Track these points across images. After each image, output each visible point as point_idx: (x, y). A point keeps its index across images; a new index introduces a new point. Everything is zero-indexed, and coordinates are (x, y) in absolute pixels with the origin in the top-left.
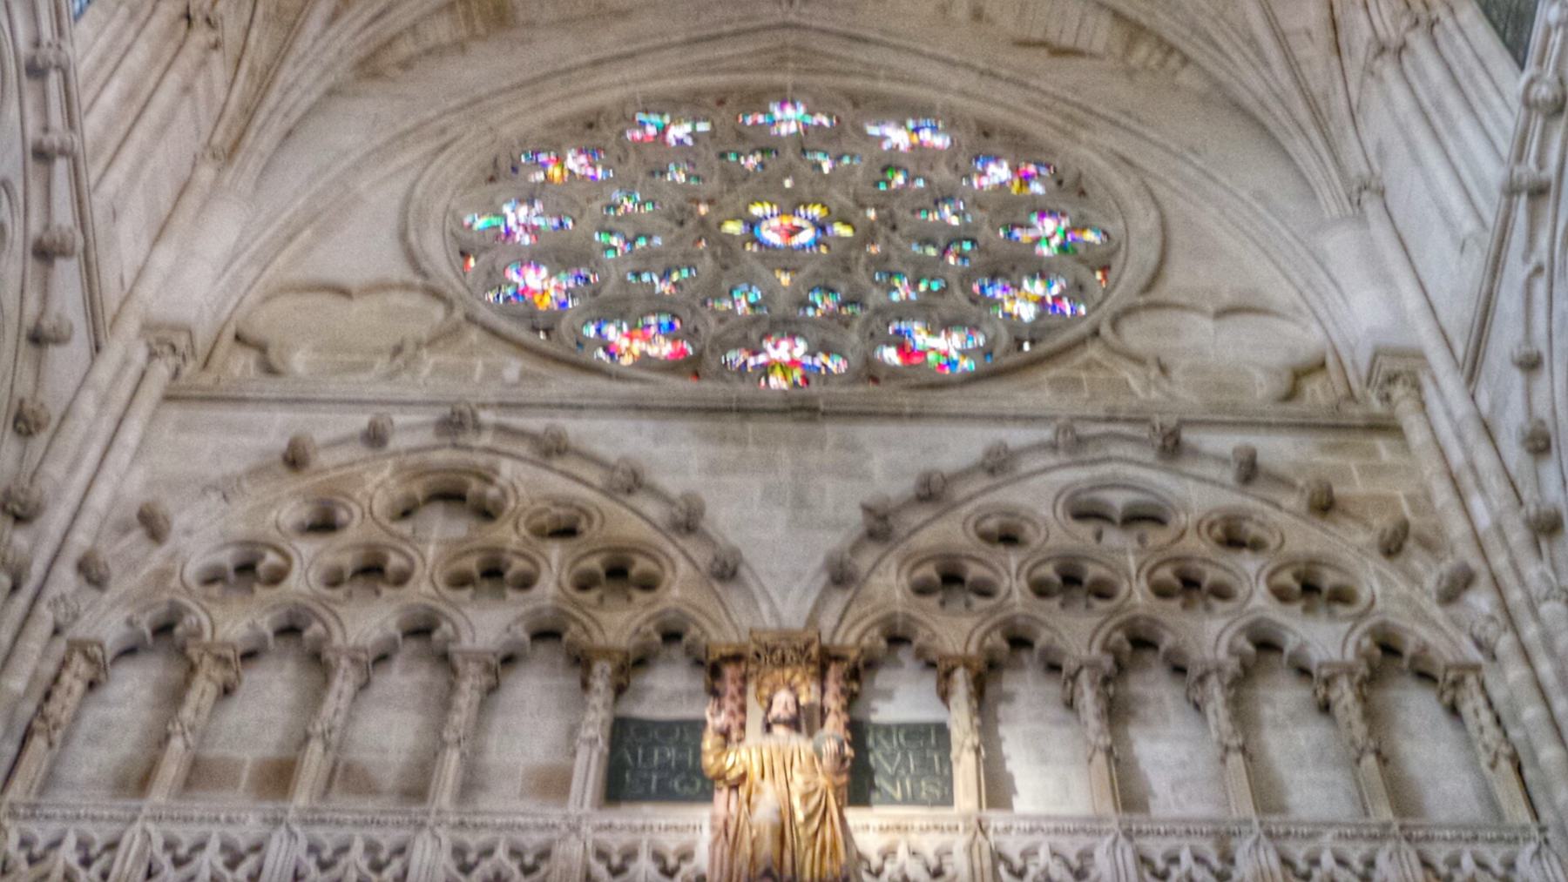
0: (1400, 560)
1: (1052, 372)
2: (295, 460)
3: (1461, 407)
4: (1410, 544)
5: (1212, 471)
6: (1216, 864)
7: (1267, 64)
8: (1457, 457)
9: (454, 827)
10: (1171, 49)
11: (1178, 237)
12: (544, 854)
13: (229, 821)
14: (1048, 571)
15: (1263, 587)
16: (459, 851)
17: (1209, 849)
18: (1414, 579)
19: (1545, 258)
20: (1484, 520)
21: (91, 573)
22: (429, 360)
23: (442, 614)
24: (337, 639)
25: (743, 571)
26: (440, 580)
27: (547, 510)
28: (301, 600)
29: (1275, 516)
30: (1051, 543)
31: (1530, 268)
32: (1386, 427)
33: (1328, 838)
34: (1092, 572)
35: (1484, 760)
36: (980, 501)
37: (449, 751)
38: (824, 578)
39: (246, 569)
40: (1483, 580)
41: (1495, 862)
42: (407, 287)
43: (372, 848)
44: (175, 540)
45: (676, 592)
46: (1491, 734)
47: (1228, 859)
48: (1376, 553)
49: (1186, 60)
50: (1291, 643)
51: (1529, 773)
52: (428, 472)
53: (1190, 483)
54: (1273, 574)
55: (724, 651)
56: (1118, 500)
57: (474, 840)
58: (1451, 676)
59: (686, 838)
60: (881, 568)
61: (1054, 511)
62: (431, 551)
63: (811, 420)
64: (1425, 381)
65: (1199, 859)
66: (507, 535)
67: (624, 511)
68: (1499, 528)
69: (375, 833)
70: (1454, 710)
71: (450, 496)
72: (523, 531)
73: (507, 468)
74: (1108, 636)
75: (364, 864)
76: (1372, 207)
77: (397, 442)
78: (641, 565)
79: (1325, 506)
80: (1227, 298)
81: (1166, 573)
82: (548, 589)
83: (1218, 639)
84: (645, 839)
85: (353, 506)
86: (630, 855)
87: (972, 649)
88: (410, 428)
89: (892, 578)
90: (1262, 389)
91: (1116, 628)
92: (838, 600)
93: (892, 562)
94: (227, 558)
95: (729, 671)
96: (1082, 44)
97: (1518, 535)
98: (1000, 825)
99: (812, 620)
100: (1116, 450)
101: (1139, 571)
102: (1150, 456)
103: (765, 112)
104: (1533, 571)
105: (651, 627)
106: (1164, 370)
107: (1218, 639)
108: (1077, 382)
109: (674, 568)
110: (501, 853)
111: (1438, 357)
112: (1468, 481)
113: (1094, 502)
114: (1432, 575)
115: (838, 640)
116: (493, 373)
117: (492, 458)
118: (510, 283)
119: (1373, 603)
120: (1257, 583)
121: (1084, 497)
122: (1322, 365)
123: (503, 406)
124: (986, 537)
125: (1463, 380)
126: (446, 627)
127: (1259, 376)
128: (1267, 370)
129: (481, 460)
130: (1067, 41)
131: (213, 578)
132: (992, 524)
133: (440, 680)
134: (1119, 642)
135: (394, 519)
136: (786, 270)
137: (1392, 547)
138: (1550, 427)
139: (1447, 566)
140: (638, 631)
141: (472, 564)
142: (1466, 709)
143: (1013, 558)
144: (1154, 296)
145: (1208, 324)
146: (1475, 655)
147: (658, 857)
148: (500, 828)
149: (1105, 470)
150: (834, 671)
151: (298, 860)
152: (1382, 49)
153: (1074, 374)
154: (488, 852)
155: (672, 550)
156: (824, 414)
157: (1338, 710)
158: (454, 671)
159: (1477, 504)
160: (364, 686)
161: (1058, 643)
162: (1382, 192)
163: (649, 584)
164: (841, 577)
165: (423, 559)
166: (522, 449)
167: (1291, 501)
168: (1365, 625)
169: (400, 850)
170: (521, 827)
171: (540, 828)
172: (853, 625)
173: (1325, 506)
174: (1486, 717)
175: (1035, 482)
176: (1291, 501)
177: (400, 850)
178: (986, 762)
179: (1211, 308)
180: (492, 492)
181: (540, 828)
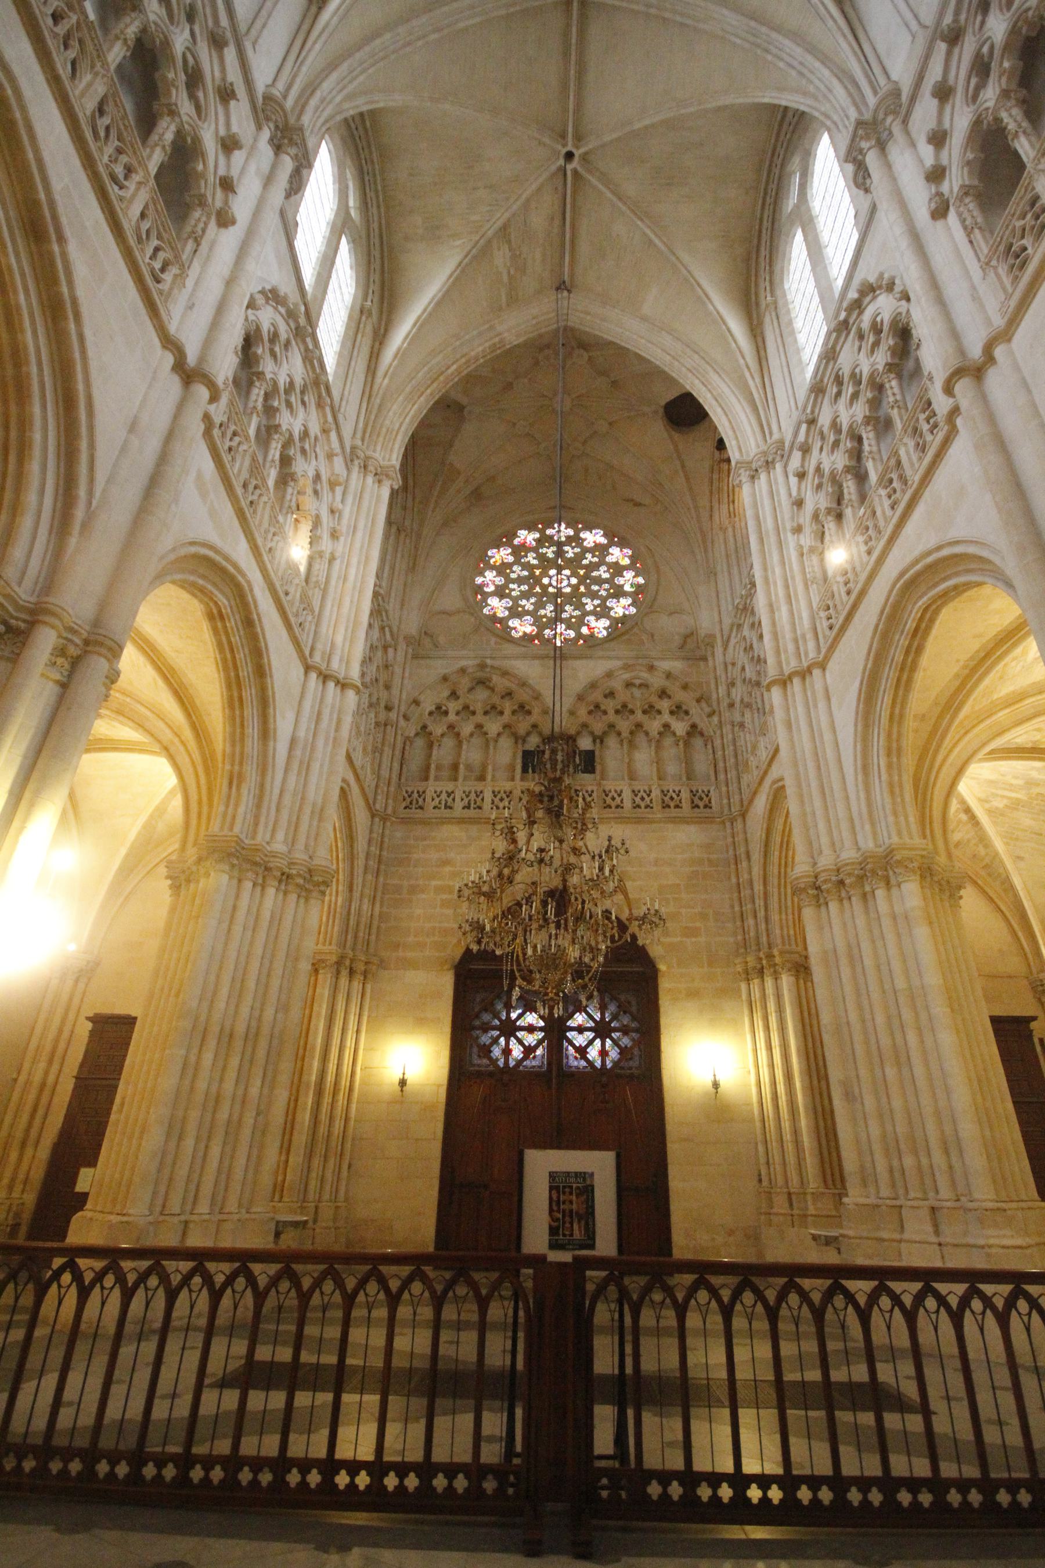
21: (406, 717)
39: (439, 708)
44: (422, 705)
56: (637, 682)
66: (496, 700)
79: (685, 687)
94: (433, 708)
131: (431, 713)
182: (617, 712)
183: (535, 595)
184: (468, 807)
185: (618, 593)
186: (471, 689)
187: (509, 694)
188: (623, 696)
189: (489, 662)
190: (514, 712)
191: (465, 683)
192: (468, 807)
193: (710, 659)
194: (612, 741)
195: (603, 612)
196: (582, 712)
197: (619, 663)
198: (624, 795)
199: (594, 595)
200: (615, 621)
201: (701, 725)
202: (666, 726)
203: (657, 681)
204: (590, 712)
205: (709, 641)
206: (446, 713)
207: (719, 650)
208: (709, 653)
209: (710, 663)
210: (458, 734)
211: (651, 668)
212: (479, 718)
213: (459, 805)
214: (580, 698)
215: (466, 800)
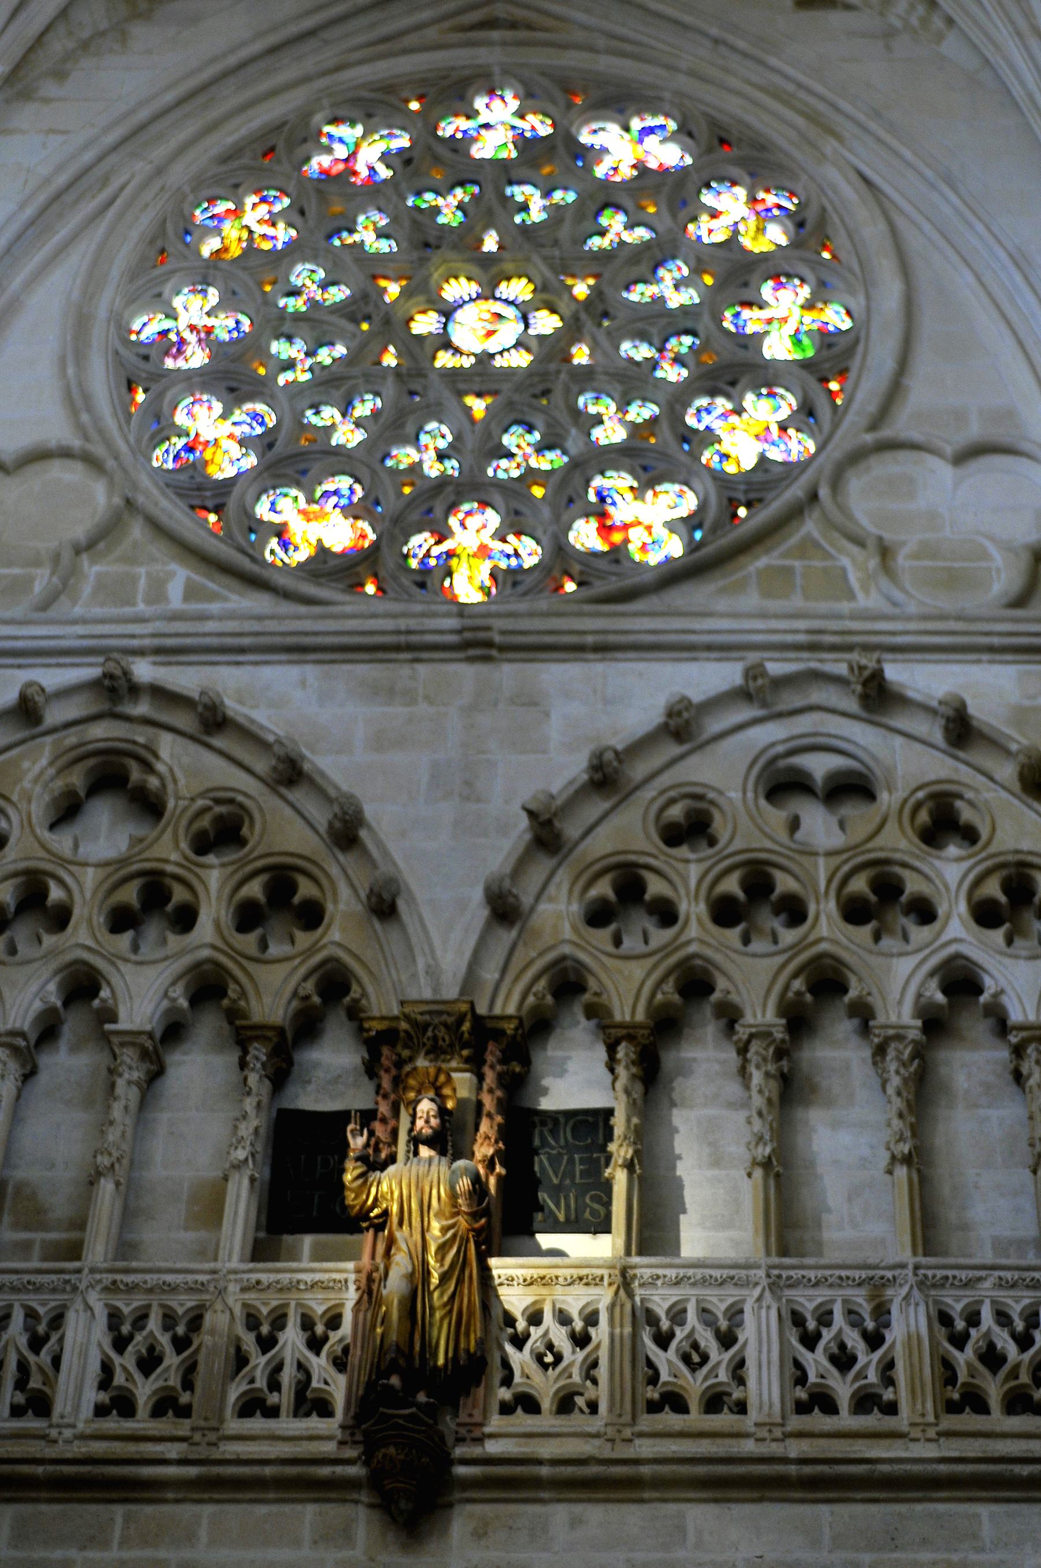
6: (870, 1325)
9: (106, 1289)
11: (928, 324)
16: (114, 1318)
17: (861, 1299)
22: (93, 570)
25: (401, 905)
26: (100, 920)
27: (208, 809)
29: (991, 794)
33: (987, 1289)
34: (784, 883)
37: (102, 1181)
38: (485, 913)
42: (65, 453)
45: (335, 934)
47: (881, 1312)
50: (990, 985)
53: (899, 741)
57: (127, 1307)
59: (333, 1298)
60: (552, 889)
61: (744, 793)
62: (90, 877)
63: (486, 659)
67: (288, 811)
72: (184, 845)
73: (167, 746)
74: (787, 987)
75: (23, 1341)
77: (55, 715)
80: (974, 431)
81: (860, 885)
83: (907, 982)
84: (292, 1299)
86: (279, 1321)
87: (640, 1016)
88: (66, 693)
89: (562, 907)
91: (795, 975)
92: (506, 936)
93: (563, 876)
98: (647, 1273)
99: (470, 981)
100: (819, 695)
101: (829, 881)
102: (852, 705)
103: (471, 114)
105: (309, 986)
106: (885, 552)
107: (907, 982)
108: (788, 572)
110: (154, 1324)
115: (497, 1011)
116: (157, 593)
117: (151, 730)
118: (182, 433)
120: (956, 903)
121: (782, 763)
123: (163, 653)
126: (105, 993)
127: (998, 558)
128: (1007, 547)
132: (676, 812)
133: (103, 1059)
134: (799, 994)
135: (52, 827)
136: (479, 395)
140: (295, 994)
141: (130, 894)
144: (886, 433)
145: (945, 471)
147: (307, 1323)
148: (151, 1291)
149: (804, 724)
150: (492, 1053)
153: (787, 562)
154: (141, 1319)
155: (334, 871)
156: (503, 648)
160: (29, 1075)
161: (734, 997)
166: (184, 720)
170: (173, 1289)
172: (516, 979)
176: (1007, 771)
178: (640, 1177)
179: (949, 450)
180: (153, 782)
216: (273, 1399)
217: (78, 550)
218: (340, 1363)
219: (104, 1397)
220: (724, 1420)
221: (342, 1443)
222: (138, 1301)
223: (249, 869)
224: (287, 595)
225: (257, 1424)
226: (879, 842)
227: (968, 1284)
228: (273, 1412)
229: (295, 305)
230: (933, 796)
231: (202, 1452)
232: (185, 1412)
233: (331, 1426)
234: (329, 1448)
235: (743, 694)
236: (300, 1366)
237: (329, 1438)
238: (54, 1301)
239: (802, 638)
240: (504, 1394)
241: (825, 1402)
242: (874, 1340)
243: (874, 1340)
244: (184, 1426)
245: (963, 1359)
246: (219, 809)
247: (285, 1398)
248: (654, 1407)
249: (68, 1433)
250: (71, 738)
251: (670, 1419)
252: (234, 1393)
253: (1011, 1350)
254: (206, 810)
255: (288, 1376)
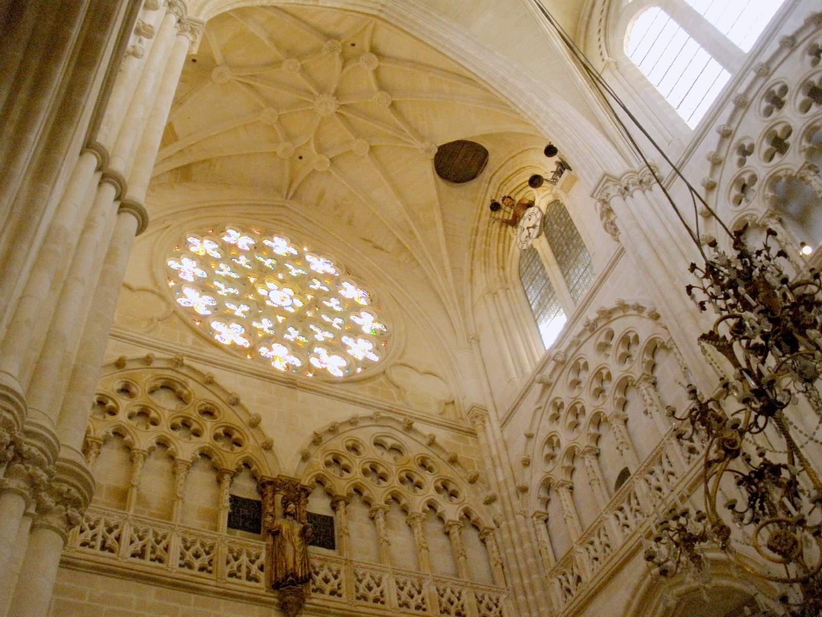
0: (473, 485)
1: (370, 384)
2: (120, 364)
3: (498, 436)
4: (478, 482)
5: (419, 439)
6: (418, 588)
7: (446, 277)
8: (494, 452)
10: (414, 259)
12: (212, 547)
13: (108, 515)
14: (367, 466)
15: (433, 487)
16: (184, 540)
17: (415, 580)
18: (477, 494)
19: (543, 405)
20: (501, 479)
23: (170, 440)
24: (137, 446)
28: (123, 424)
30: (369, 456)
31: (537, 406)
32: (473, 433)
35: (492, 563)
36: (347, 434)
40: (499, 500)
41: (494, 599)
42: (153, 292)
43: (156, 534)
46: (495, 555)
47: (421, 586)
48: (466, 481)
49: (418, 265)
51: (506, 570)
52: (161, 379)
54: (436, 481)
55: (267, 479)
56: (390, 442)
57: (190, 539)
58: (486, 531)
62: (167, 414)
64: (486, 419)
65: (413, 585)
67: (232, 412)
68: (505, 481)
69: (157, 529)
70: (483, 541)
71: (168, 386)
73: (192, 385)
76: (475, 347)
78: (236, 435)
79: (453, 461)
81: (403, 475)
82: (206, 439)
85: (139, 388)
90: (434, 409)
95: (269, 487)
96: (384, 247)
97: (512, 489)
104: (516, 503)
109: (248, 439)
110: (198, 545)
111: (492, 414)
112: (497, 462)
113: (381, 440)
114: (484, 496)
118: (186, 297)
119: (464, 500)
122: (453, 402)
124: (348, 448)
125: (500, 425)
129: (182, 378)
130: (379, 243)
132: (350, 444)
137: (472, 481)
138: (531, 458)
139: (490, 493)
141: (178, 421)
142: (488, 543)
143: (358, 460)
146: (493, 526)
149: (386, 430)
151: (132, 535)
152: (490, 292)
154: (193, 543)
155: (248, 433)
157: (452, 537)
158: (175, 466)
159: (499, 470)
161: (371, 496)
162: (478, 341)
163: (238, 443)
164: (305, 457)
165: (164, 417)
167: (443, 456)
168: (462, 508)
169: (164, 537)
170: (205, 537)
171: (212, 538)
173: (453, 461)
174: (495, 548)
175: (364, 430)
177: (164, 537)
180: (185, 392)
181: (212, 538)
182: (365, 472)
183: (247, 302)
184: (141, 555)
185: (355, 332)
186: (152, 392)
187: (208, 413)
188: (371, 453)
189: (186, 361)
190: (216, 437)
191: (145, 379)
192: (141, 555)
193: (480, 434)
194: (358, 510)
195: (335, 347)
196: (318, 460)
197: (370, 412)
198: (384, 584)
199: (327, 327)
200: (353, 363)
201: (476, 514)
202: (432, 506)
203: (414, 448)
204: (328, 464)
205: (478, 414)
206: (112, 412)
207: (493, 425)
208: (478, 429)
209: (482, 440)
210: (128, 448)
211: (409, 428)
212: (164, 429)
213: (126, 549)
214: (317, 440)
215: (138, 545)
216: (239, 574)
217: (159, 320)
218: (261, 568)
219: (182, 562)
220: (379, 605)
221: (267, 591)
222: (193, 538)
223: (219, 425)
224: (227, 352)
225: (234, 580)
226: (408, 465)
227: (444, 582)
228: (240, 578)
229: (223, 274)
230: (423, 457)
231: (220, 585)
232: (210, 572)
233: (263, 584)
234: (263, 592)
235: (371, 418)
236: (247, 567)
237: (262, 589)
238: (165, 531)
239: (387, 408)
240: (312, 587)
241: (406, 605)
242: (419, 592)
243: (419, 592)
244: (212, 576)
245: (444, 600)
246: (208, 406)
247: (243, 574)
248: (358, 598)
249: (175, 571)
250: (160, 372)
251: (362, 602)
252: (228, 570)
253: (456, 600)
254: (203, 404)
255: (244, 569)
